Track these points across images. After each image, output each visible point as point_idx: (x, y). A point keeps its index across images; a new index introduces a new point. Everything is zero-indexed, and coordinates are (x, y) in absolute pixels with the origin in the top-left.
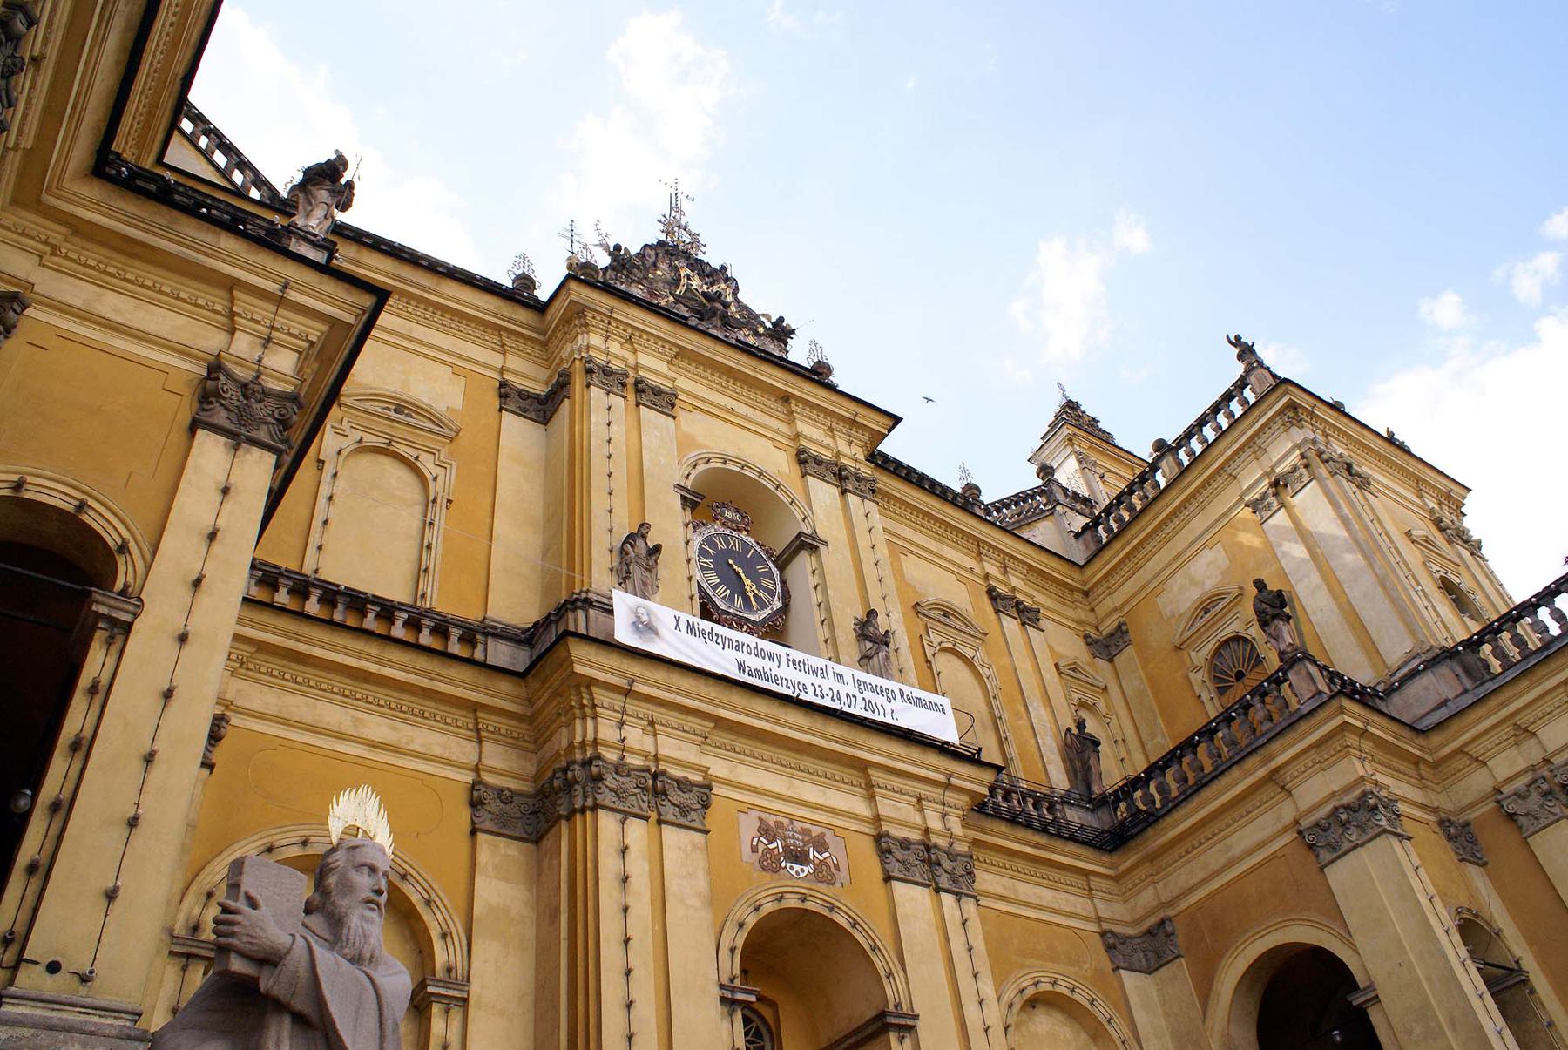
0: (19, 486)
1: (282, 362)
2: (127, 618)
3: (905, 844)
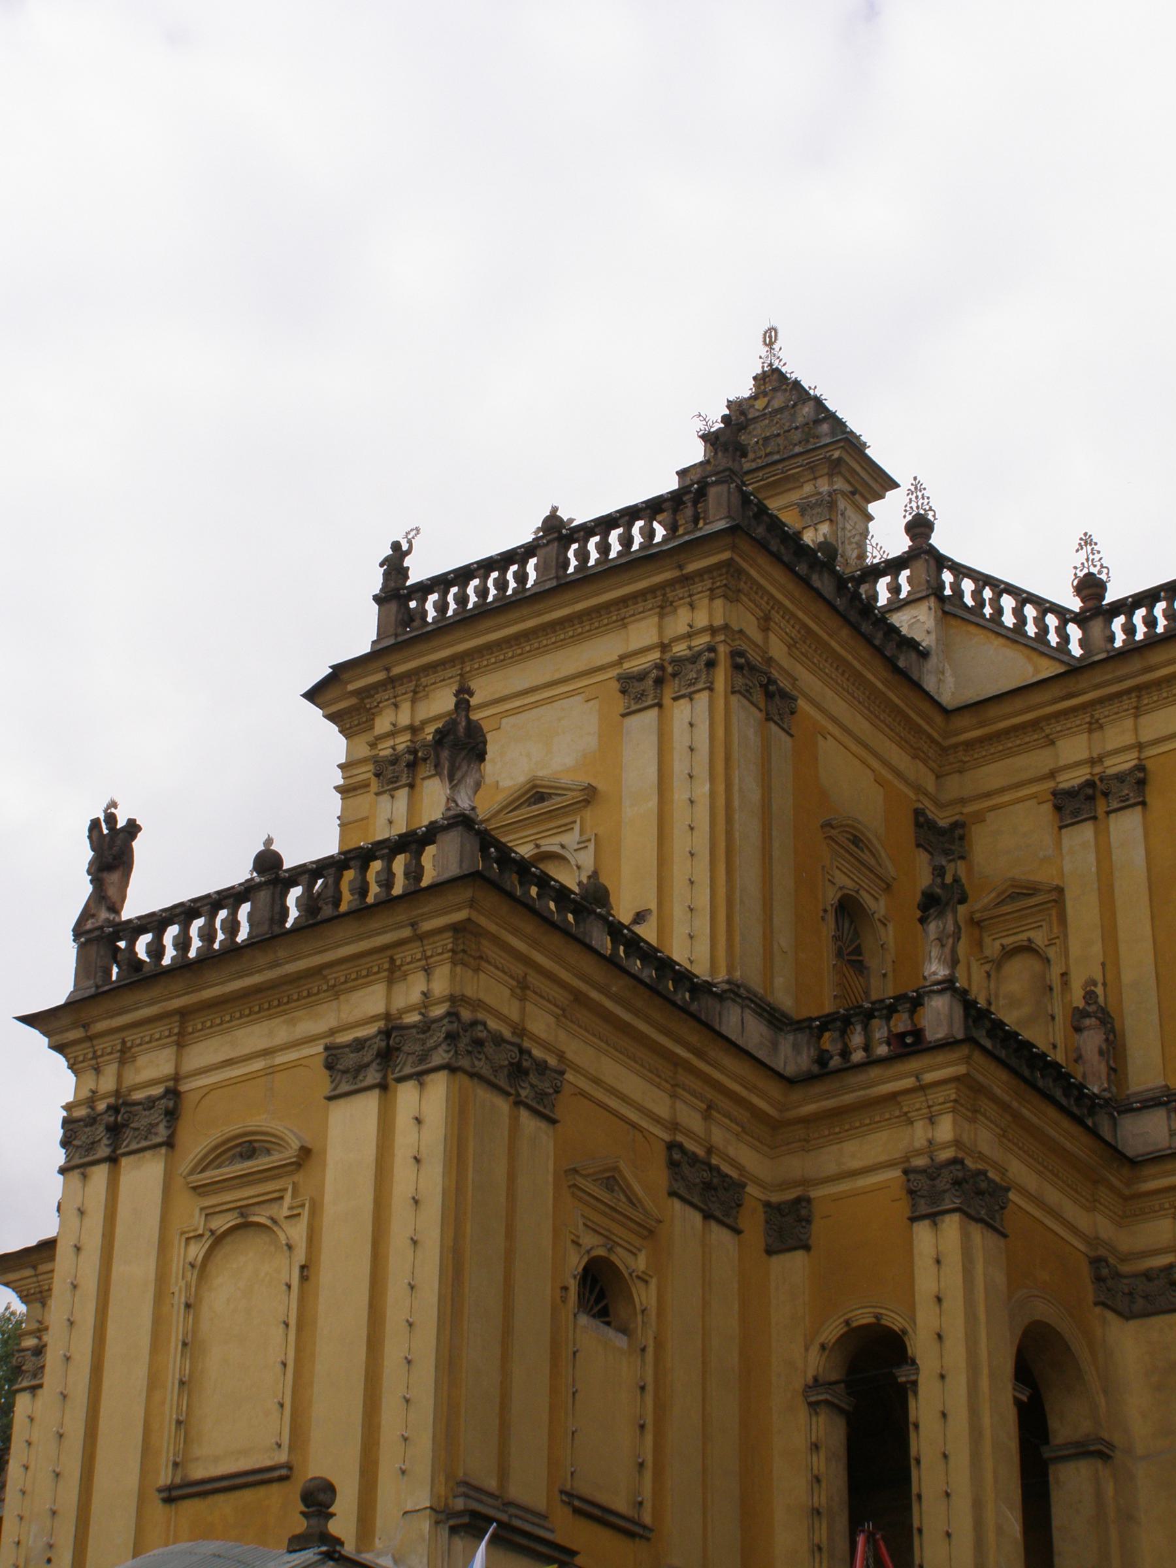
0: (847, 1322)
1: (945, 1130)
2: (913, 1378)
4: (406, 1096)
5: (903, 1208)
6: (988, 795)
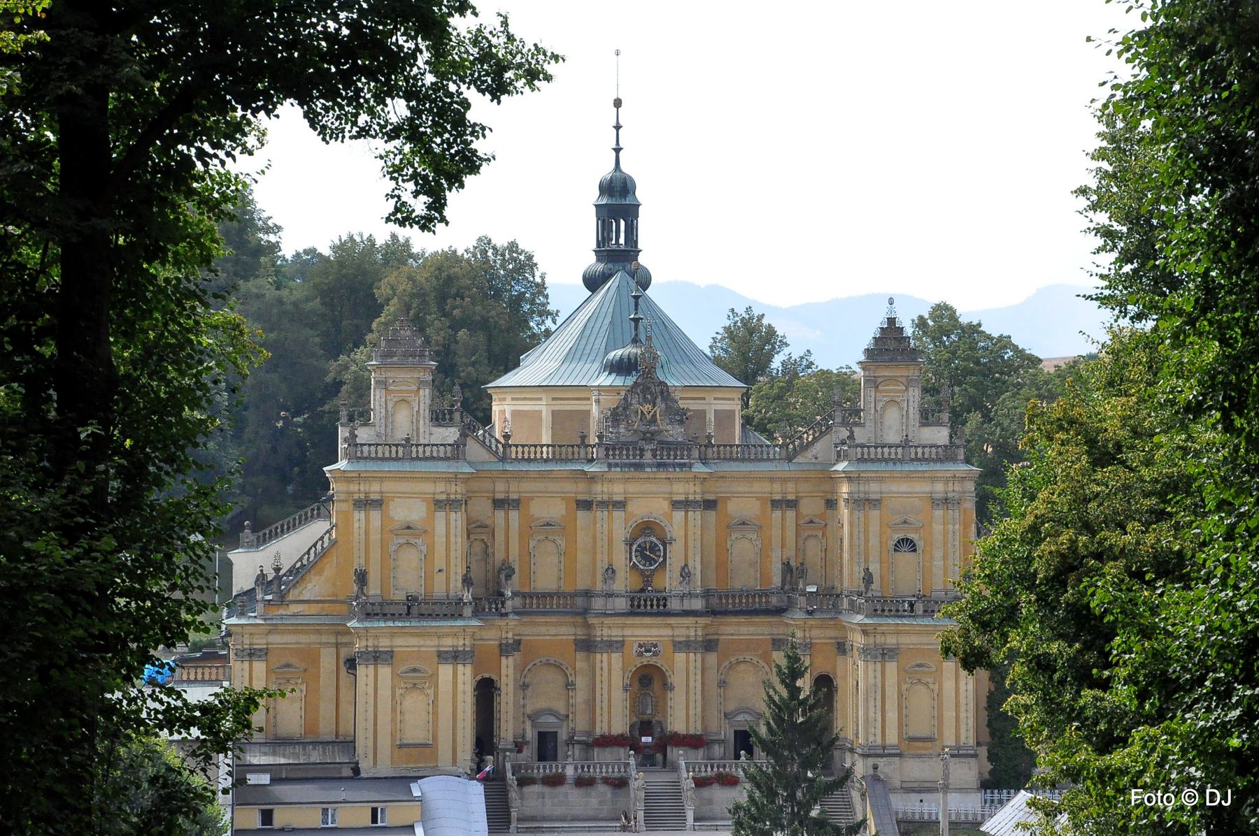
3: (680, 642)
4: (460, 667)
5: (497, 651)
6: (473, 492)
